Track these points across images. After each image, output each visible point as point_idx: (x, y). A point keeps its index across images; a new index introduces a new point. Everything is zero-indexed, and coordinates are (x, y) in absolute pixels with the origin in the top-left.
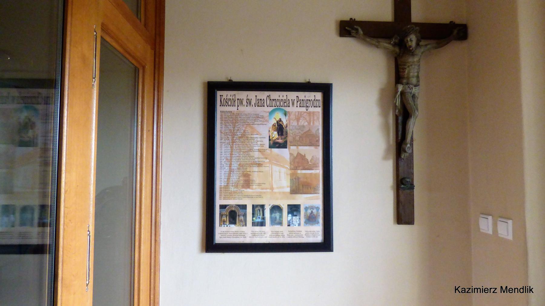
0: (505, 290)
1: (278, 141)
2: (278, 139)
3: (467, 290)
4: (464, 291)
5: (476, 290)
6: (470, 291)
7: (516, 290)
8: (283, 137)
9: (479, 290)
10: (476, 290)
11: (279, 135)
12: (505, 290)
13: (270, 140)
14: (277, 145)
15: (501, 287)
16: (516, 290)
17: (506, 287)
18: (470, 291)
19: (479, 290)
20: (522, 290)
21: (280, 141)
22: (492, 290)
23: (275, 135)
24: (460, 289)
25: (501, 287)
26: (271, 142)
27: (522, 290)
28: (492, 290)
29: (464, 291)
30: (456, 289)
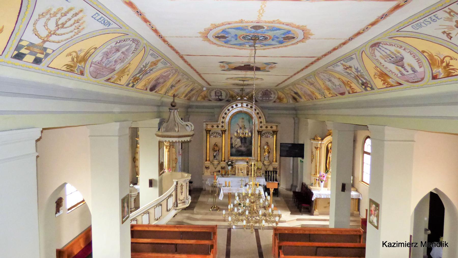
1: (241, 148)
2: (240, 147)
3: (392, 245)
4: (390, 245)
5: (400, 244)
6: (396, 245)
8: (246, 145)
10: (400, 244)
11: (242, 142)
13: (232, 147)
14: (240, 153)
15: (422, 242)
18: (396, 245)
21: (243, 149)
23: (238, 142)
24: (387, 244)
25: (422, 242)
26: (234, 150)
29: (390, 245)
30: (384, 244)
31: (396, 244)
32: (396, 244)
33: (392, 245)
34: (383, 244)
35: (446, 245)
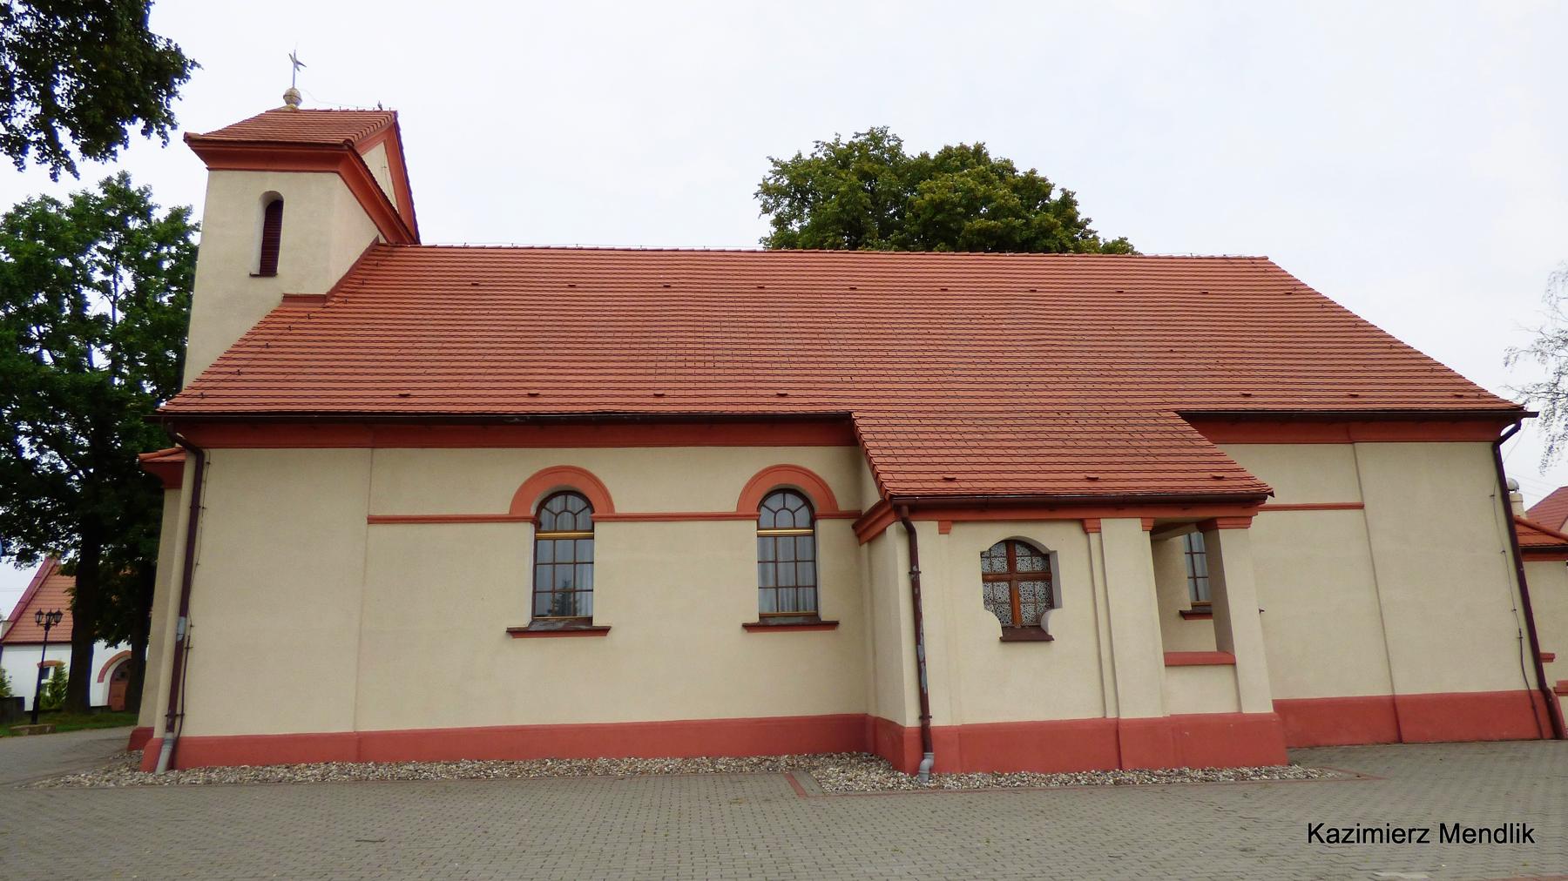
0: (1453, 834)
3: (1343, 834)
4: (1334, 837)
5: (1369, 834)
6: (1354, 836)
7: (1485, 834)
9: (1377, 834)
10: (1369, 834)
12: (1453, 834)
15: (1443, 826)
16: (1485, 834)
17: (1457, 826)
18: (1354, 836)
19: (1377, 834)
20: (1500, 836)
22: (1416, 835)
24: (1323, 832)
25: (1443, 826)
27: (1500, 836)
28: (1416, 835)
29: (1334, 837)
30: (1312, 832)
31: (1354, 834)
32: (1354, 834)
33: (1343, 834)
34: (1311, 834)
35: (1525, 835)
